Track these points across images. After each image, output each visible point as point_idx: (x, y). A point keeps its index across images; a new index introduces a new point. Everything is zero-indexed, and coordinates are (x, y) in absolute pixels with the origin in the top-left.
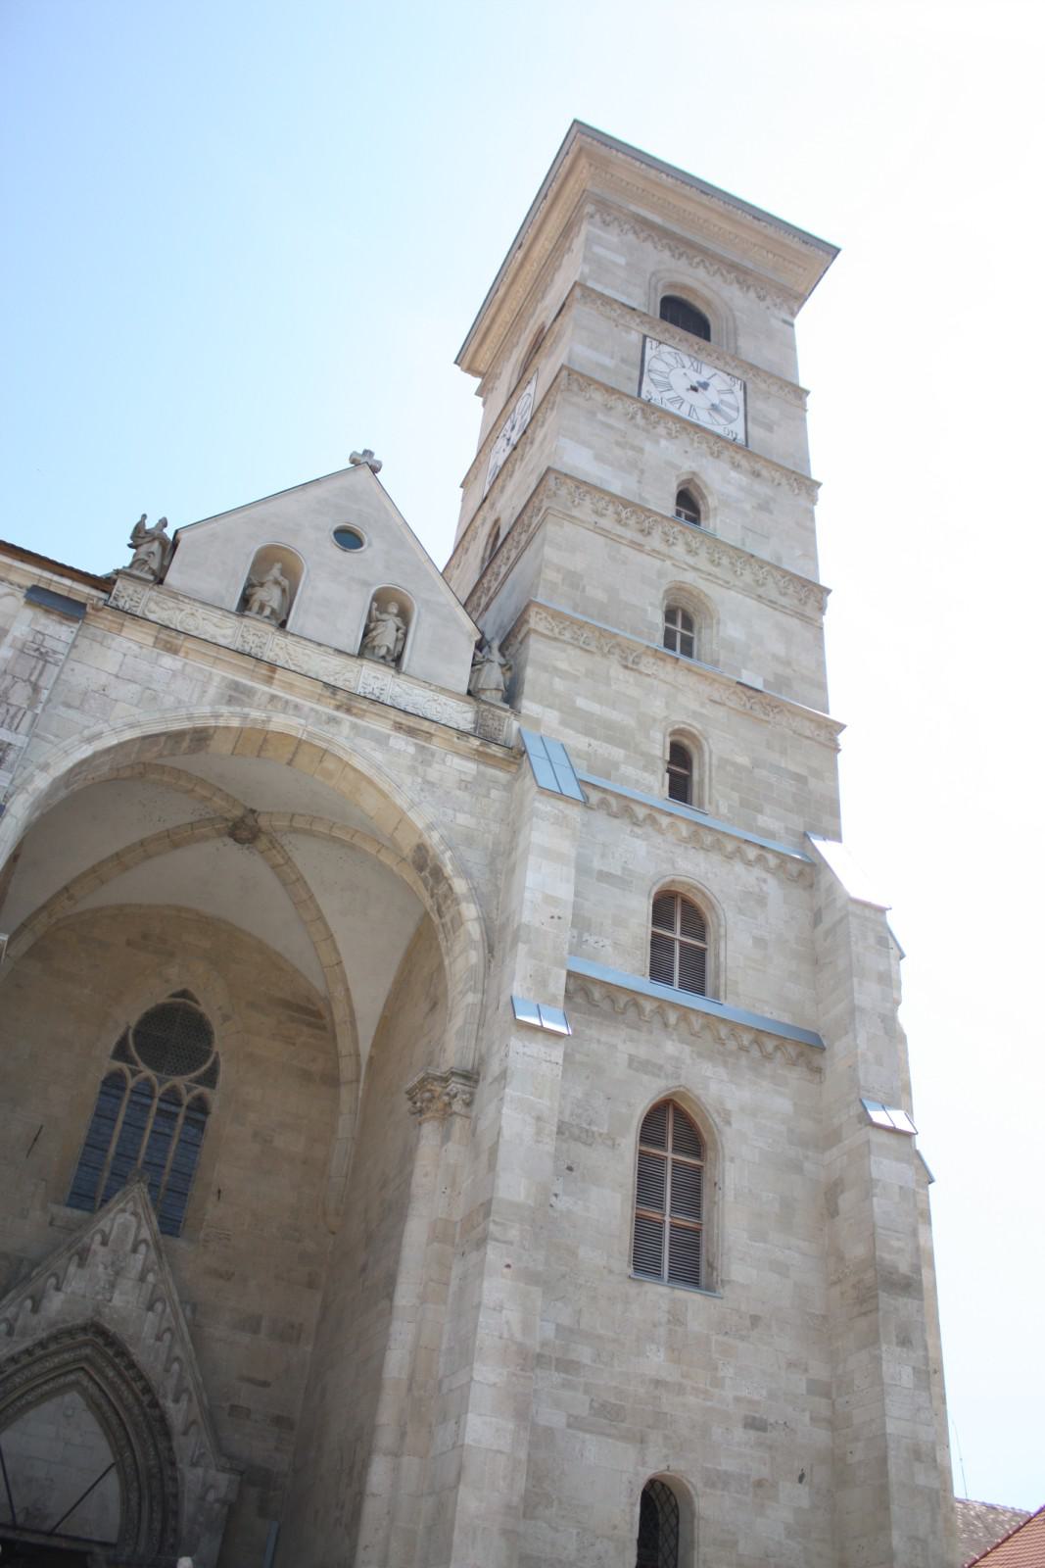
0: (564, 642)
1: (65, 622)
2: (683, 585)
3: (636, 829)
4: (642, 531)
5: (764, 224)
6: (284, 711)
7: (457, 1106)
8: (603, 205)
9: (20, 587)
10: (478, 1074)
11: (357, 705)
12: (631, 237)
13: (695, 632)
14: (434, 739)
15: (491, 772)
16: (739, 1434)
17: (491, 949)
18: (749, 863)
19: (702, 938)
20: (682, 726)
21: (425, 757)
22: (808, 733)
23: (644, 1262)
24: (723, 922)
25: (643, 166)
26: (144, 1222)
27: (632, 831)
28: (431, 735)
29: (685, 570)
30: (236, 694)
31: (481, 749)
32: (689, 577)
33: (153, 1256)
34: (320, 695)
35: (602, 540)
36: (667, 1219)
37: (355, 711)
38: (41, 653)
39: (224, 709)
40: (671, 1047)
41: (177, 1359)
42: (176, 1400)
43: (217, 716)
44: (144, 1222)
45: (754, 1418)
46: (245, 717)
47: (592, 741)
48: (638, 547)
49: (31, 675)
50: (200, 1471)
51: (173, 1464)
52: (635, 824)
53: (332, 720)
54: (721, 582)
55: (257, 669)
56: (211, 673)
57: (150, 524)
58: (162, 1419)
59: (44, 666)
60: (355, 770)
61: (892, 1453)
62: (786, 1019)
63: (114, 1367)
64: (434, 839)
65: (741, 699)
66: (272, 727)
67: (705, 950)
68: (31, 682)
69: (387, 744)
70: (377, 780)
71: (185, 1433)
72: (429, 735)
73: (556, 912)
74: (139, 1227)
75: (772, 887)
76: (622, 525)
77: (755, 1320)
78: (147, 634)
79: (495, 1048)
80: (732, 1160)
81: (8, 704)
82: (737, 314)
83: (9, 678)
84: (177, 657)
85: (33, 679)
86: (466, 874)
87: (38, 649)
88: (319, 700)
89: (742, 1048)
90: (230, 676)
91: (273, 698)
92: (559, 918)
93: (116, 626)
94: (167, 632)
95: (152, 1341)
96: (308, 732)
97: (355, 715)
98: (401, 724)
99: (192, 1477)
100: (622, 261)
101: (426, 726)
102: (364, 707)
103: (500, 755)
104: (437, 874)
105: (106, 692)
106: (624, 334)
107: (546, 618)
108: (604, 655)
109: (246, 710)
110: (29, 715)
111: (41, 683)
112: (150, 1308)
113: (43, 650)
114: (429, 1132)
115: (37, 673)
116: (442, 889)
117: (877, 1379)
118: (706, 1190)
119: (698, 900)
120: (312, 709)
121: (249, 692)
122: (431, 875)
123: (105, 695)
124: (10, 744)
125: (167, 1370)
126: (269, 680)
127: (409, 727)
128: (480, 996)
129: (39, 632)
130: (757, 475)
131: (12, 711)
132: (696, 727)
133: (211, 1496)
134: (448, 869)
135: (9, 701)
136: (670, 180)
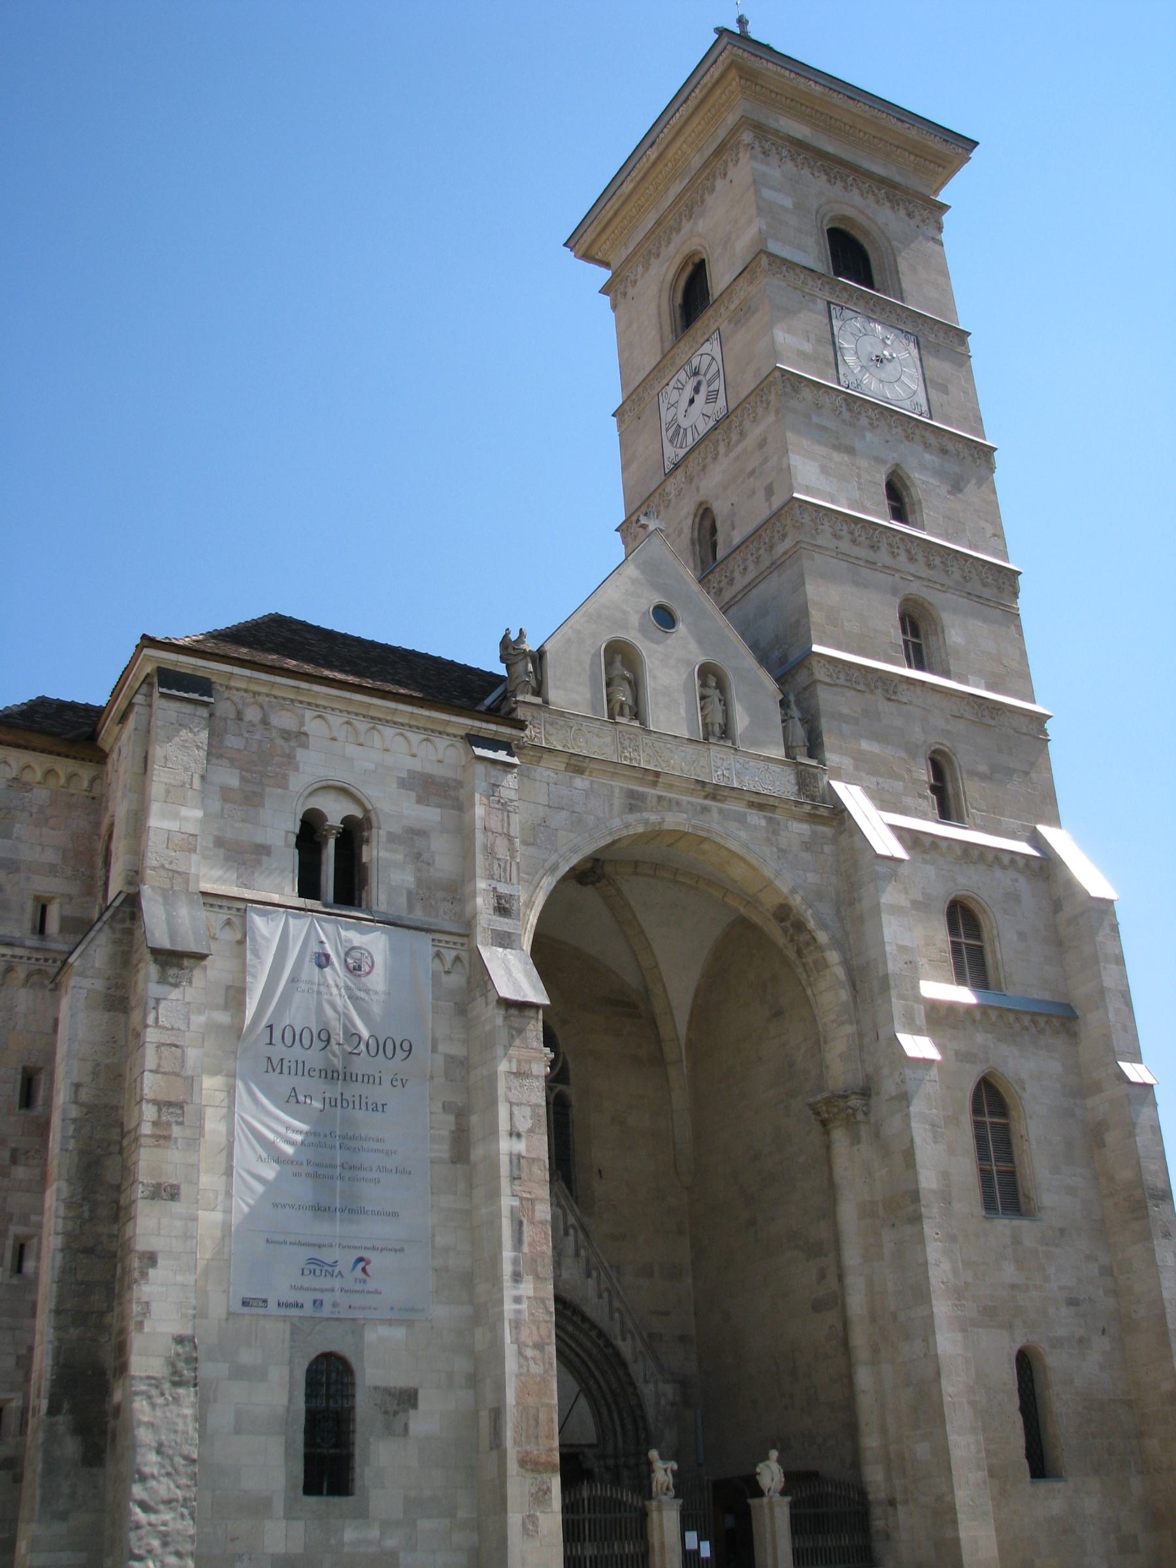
0: (842, 686)
1: (508, 770)
2: (910, 597)
3: (927, 857)
4: (872, 547)
5: (907, 125)
6: (670, 810)
7: (860, 1117)
8: (760, 129)
9: (455, 736)
10: (870, 1089)
11: (720, 793)
12: (790, 165)
13: (922, 636)
14: (777, 810)
15: (821, 829)
16: (1064, 1311)
17: (853, 985)
18: (1004, 868)
19: (982, 942)
20: (937, 746)
21: (774, 827)
22: (1024, 730)
23: (989, 1204)
24: (995, 925)
25: (793, 75)
26: (568, 1211)
27: (923, 859)
28: (775, 807)
29: (911, 581)
30: (634, 802)
31: (812, 812)
32: (916, 589)
33: (581, 1236)
34: (693, 789)
35: (844, 565)
36: (994, 1168)
37: (719, 797)
38: (502, 804)
39: (631, 818)
40: (980, 1038)
41: (618, 1310)
42: (624, 1339)
43: (627, 827)
44: (568, 1211)
45: (1071, 1298)
46: (646, 822)
47: (881, 780)
48: (871, 564)
49: (503, 828)
50: (651, 1386)
51: (632, 1384)
52: (925, 852)
53: (705, 809)
54: (938, 586)
55: (645, 777)
56: (611, 786)
57: (514, 636)
58: (617, 1354)
59: (508, 816)
60: (729, 850)
61: (1168, 1310)
62: (1047, 996)
63: (574, 1324)
64: (796, 901)
65: (973, 707)
66: (666, 826)
67: (982, 947)
68: (505, 834)
69: (746, 822)
70: (747, 857)
71: (636, 1361)
72: (773, 808)
73: (907, 958)
74: (565, 1215)
75: (1023, 886)
76: (856, 545)
77: (1062, 1230)
78: (560, 762)
79: (886, 1071)
80: (1031, 1118)
81: (498, 859)
82: (895, 243)
83: (490, 833)
84: (583, 776)
85: (505, 831)
86: (824, 927)
87: (499, 801)
88: (692, 793)
89: (1027, 1029)
90: (625, 785)
91: (660, 798)
92: (911, 962)
93: (535, 759)
94: (576, 758)
95: (596, 1300)
96: (693, 825)
97: (719, 801)
98: (753, 802)
99: (647, 1390)
100: (788, 203)
101: (771, 801)
102: (726, 794)
103: (825, 814)
104: (800, 926)
105: (547, 823)
107: (824, 665)
108: (872, 692)
109: (645, 815)
110: (513, 863)
111: (512, 834)
112: (589, 1275)
113: (502, 801)
114: (839, 1136)
115: (506, 824)
116: (804, 937)
117: (1151, 1261)
118: (1015, 1140)
119: (973, 906)
120: (689, 802)
121: (641, 797)
122: (793, 925)
123: (546, 826)
124: (511, 895)
125: (612, 1318)
126: (655, 784)
127: (760, 804)
128: (855, 1026)
129: (494, 785)
130: (944, 451)
131: (502, 865)
132: (946, 744)
133: (663, 1402)
134: (811, 924)
135: (497, 856)
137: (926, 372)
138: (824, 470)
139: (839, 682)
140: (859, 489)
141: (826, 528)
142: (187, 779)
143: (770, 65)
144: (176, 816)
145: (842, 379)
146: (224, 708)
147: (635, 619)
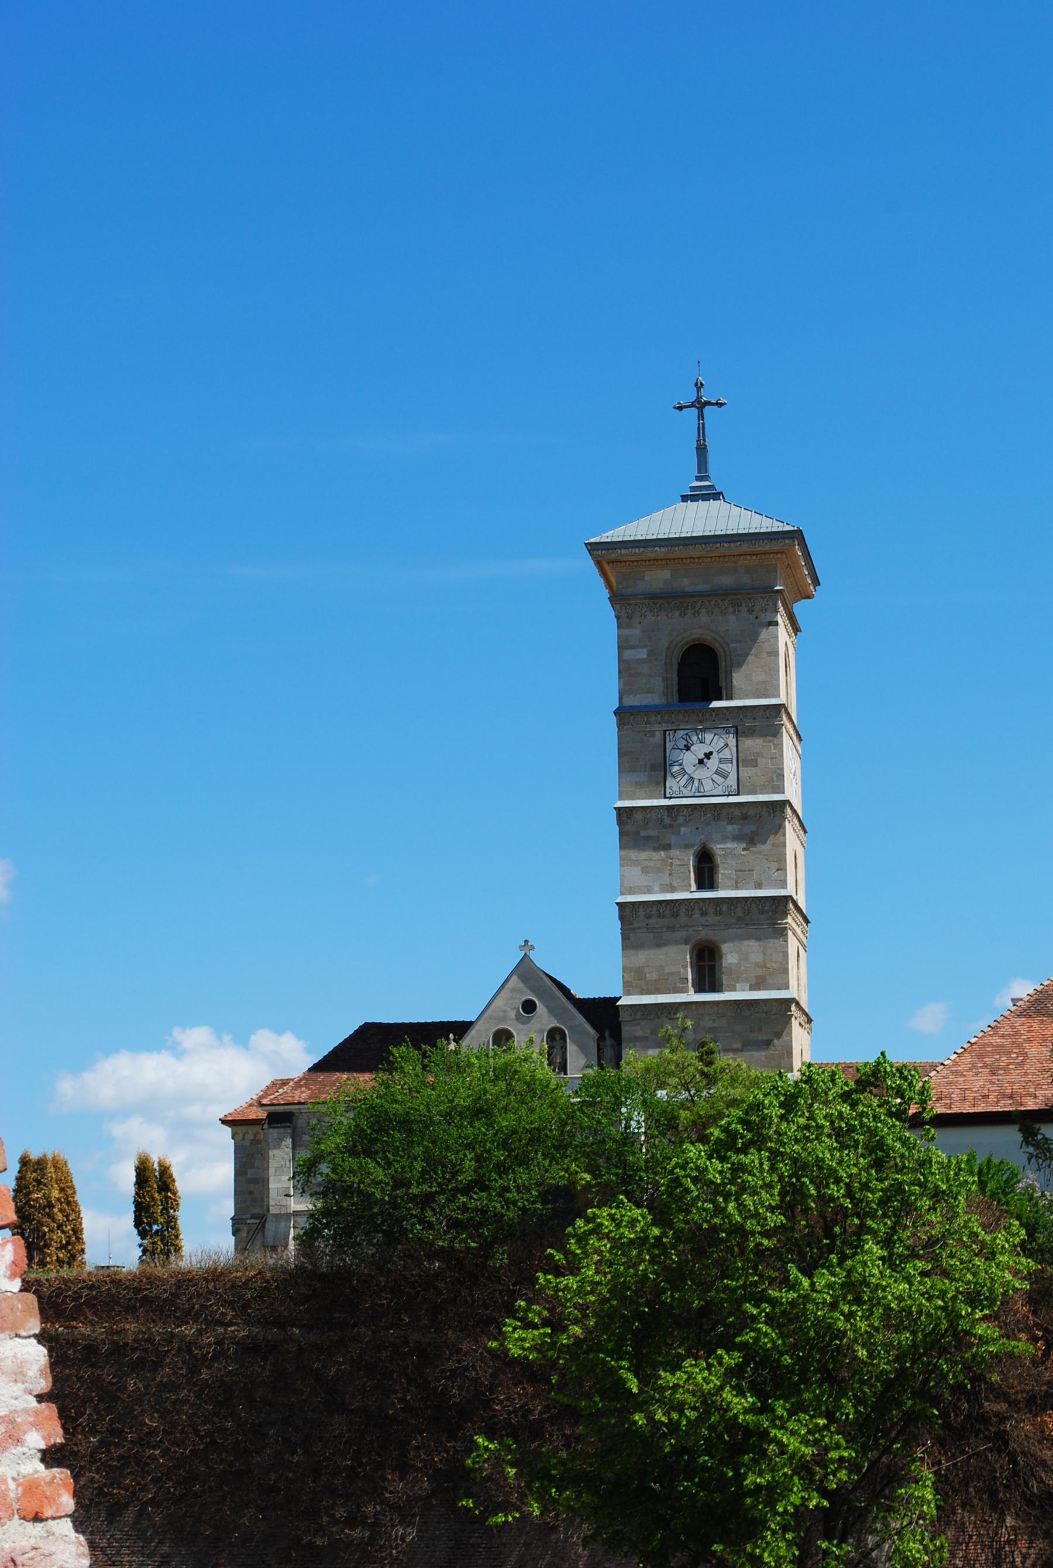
25: (642, 549)
32: (704, 934)
35: (651, 935)
48: (671, 928)
100: (642, 654)
106: (651, 739)
108: (658, 1018)
136: (663, 550)
137: (740, 755)
138: (645, 871)
139: (638, 1017)
140: (670, 874)
141: (642, 913)
142: (283, 1163)
143: (624, 551)
144: (280, 1181)
145: (668, 791)
146: (301, 1122)
147: (512, 1014)
